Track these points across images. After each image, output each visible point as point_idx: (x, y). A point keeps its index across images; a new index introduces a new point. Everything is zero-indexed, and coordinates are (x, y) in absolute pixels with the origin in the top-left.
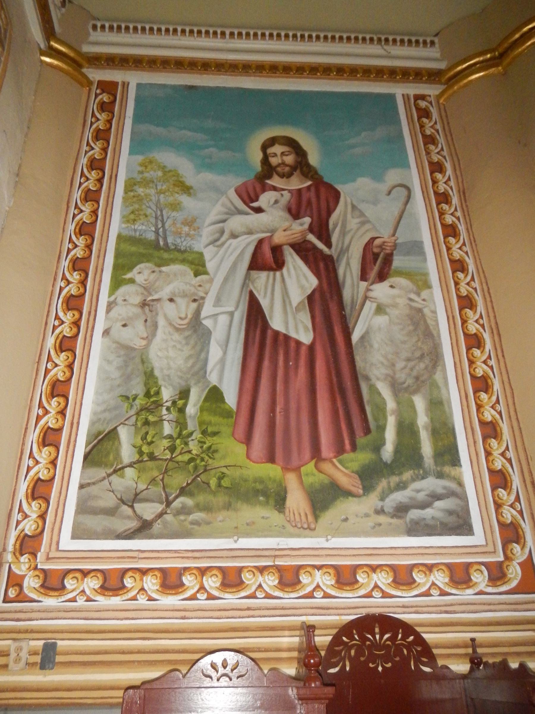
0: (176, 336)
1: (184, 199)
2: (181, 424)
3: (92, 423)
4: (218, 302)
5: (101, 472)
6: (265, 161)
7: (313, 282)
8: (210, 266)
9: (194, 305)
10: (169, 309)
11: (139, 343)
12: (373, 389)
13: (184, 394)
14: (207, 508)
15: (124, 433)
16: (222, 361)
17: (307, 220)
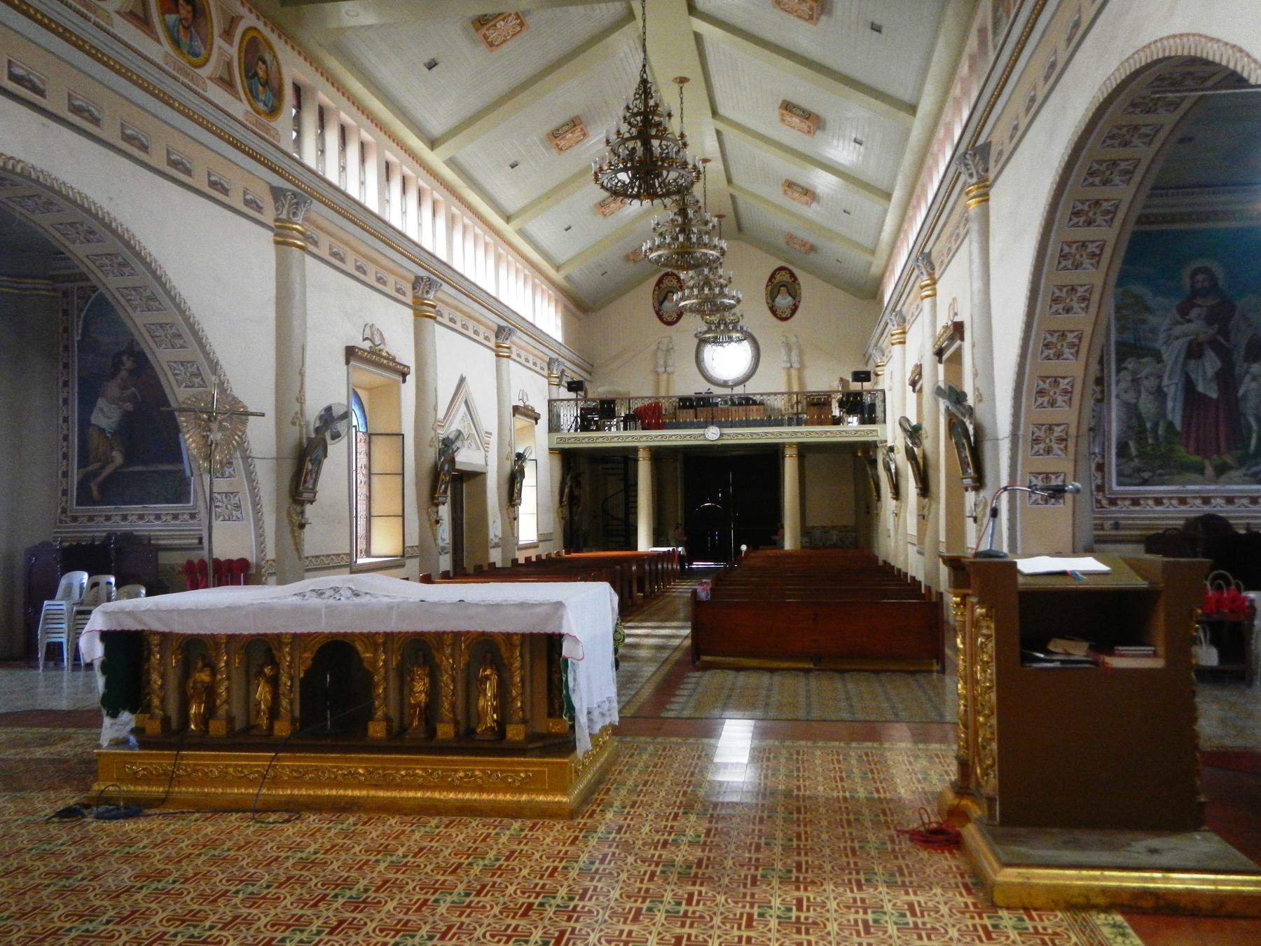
0: (1151, 397)
1: (1150, 318)
2: (1156, 438)
3: (1118, 438)
4: (1170, 379)
5: (1124, 461)
6: (1192, 286)
7: (1219, 364)
8: (1165, 357)
9: (1158, 380)
10: (1146, 382)
11: (1133, 401)
12: (1248, 423)
13: (1156, 425)
14: (1170, 474)
15: (1131, 444)
16: (1174, 409)
17: (1216, 326)
